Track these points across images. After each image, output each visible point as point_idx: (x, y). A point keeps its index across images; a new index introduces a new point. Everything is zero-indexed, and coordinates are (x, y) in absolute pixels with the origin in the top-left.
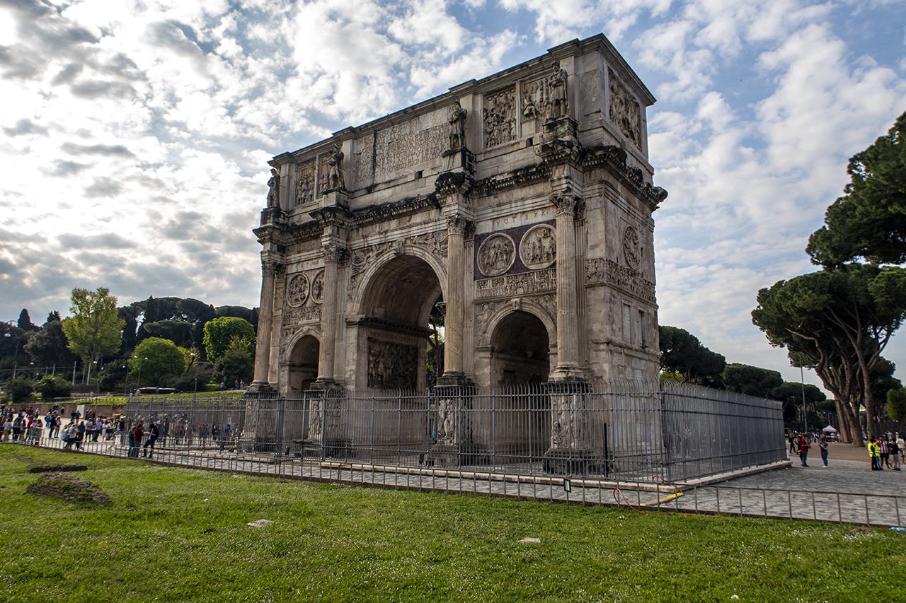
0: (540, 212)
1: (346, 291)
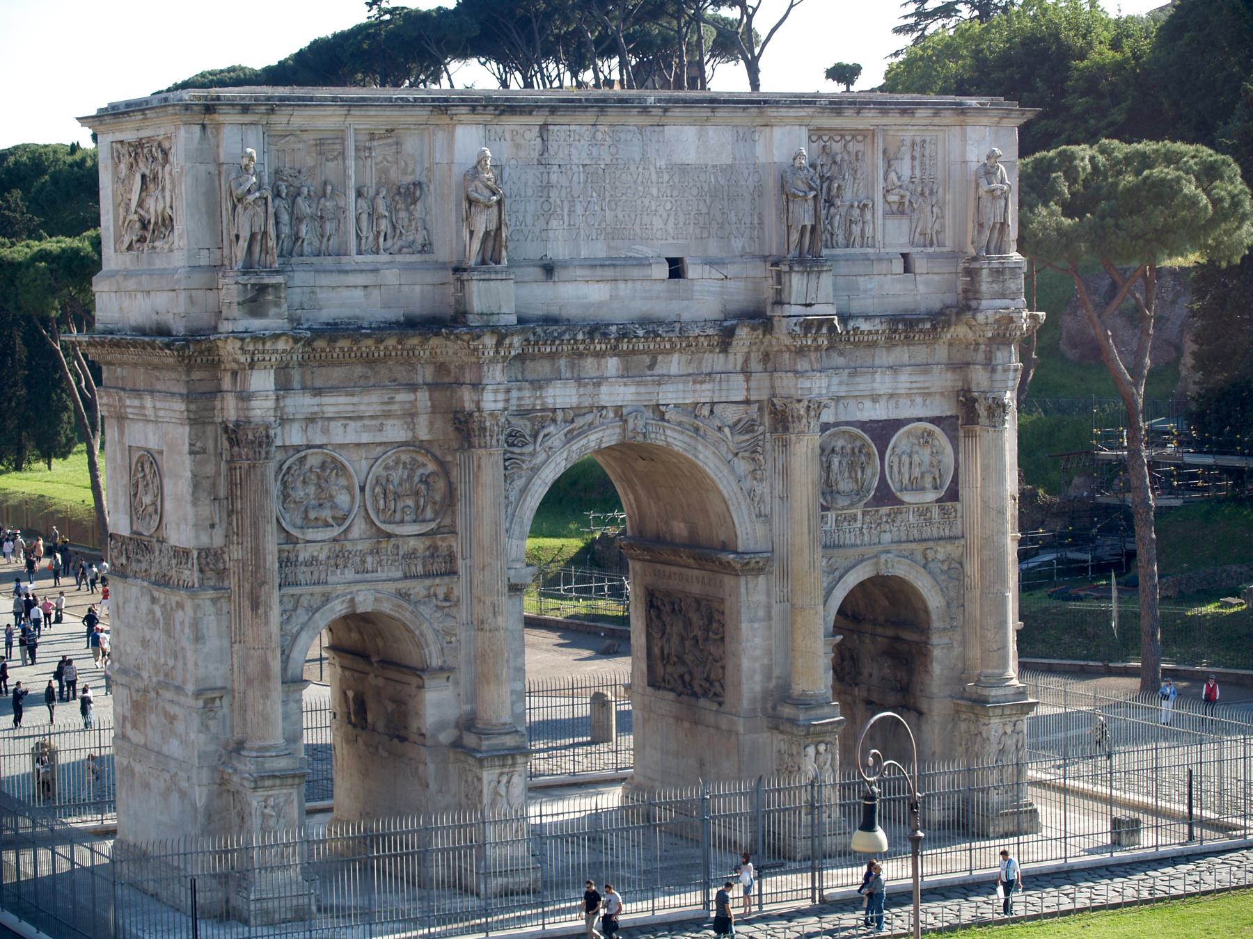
0: (919, 400)
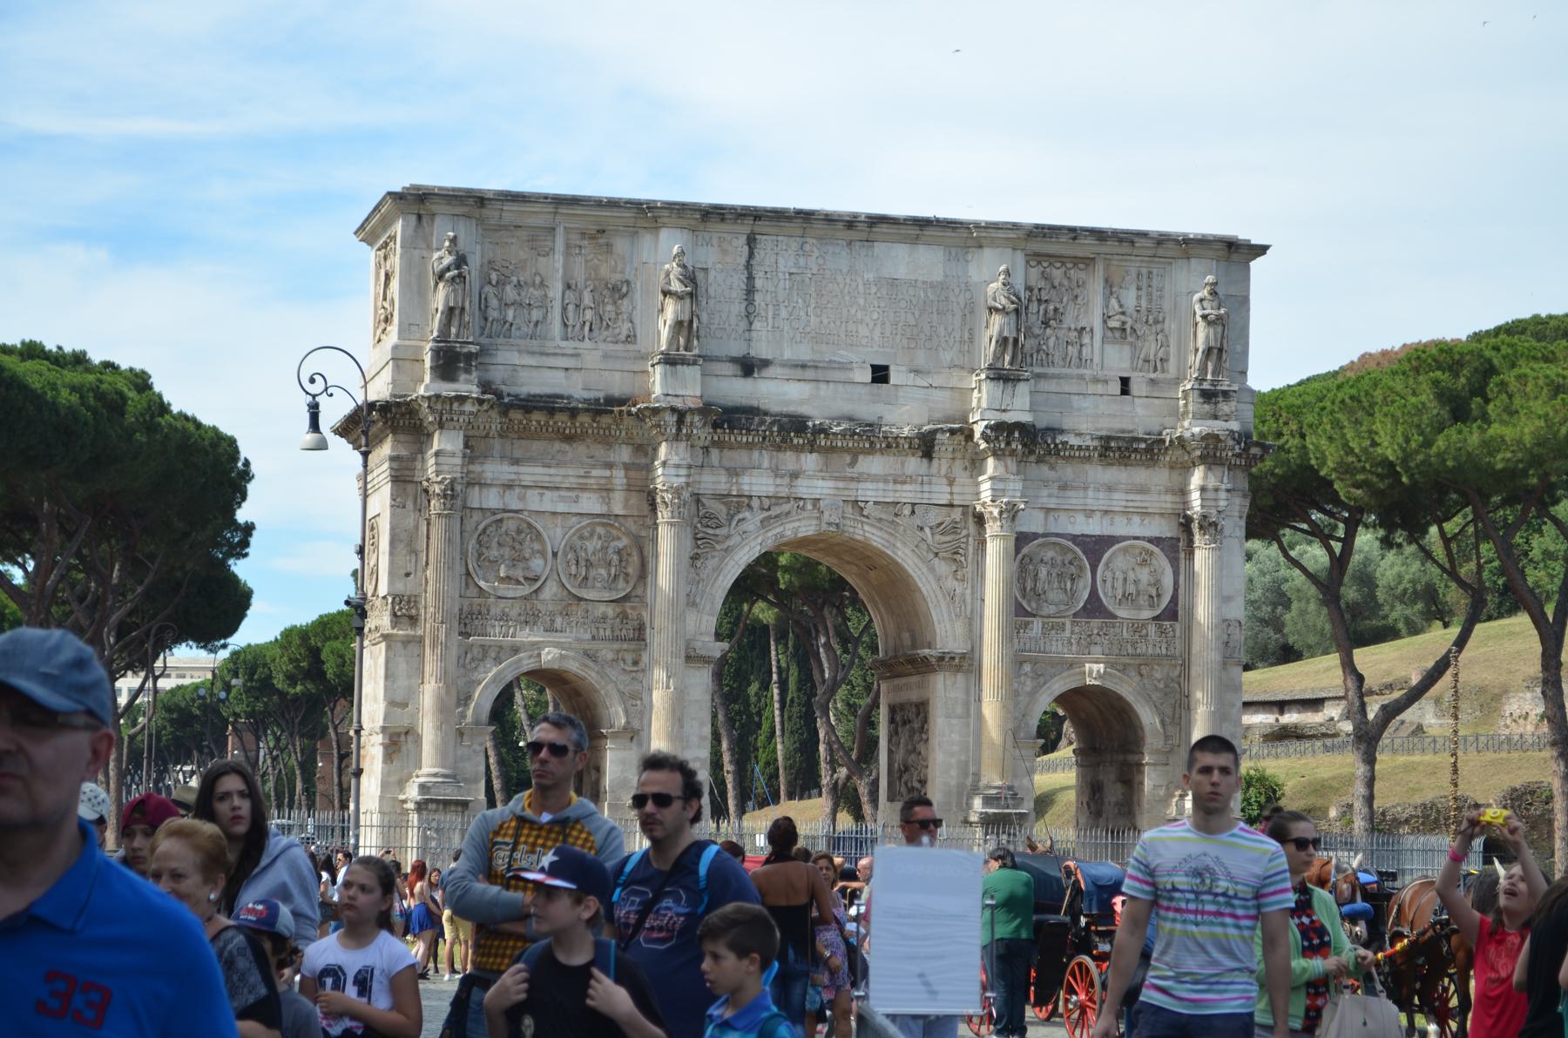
0: (1136, 519)
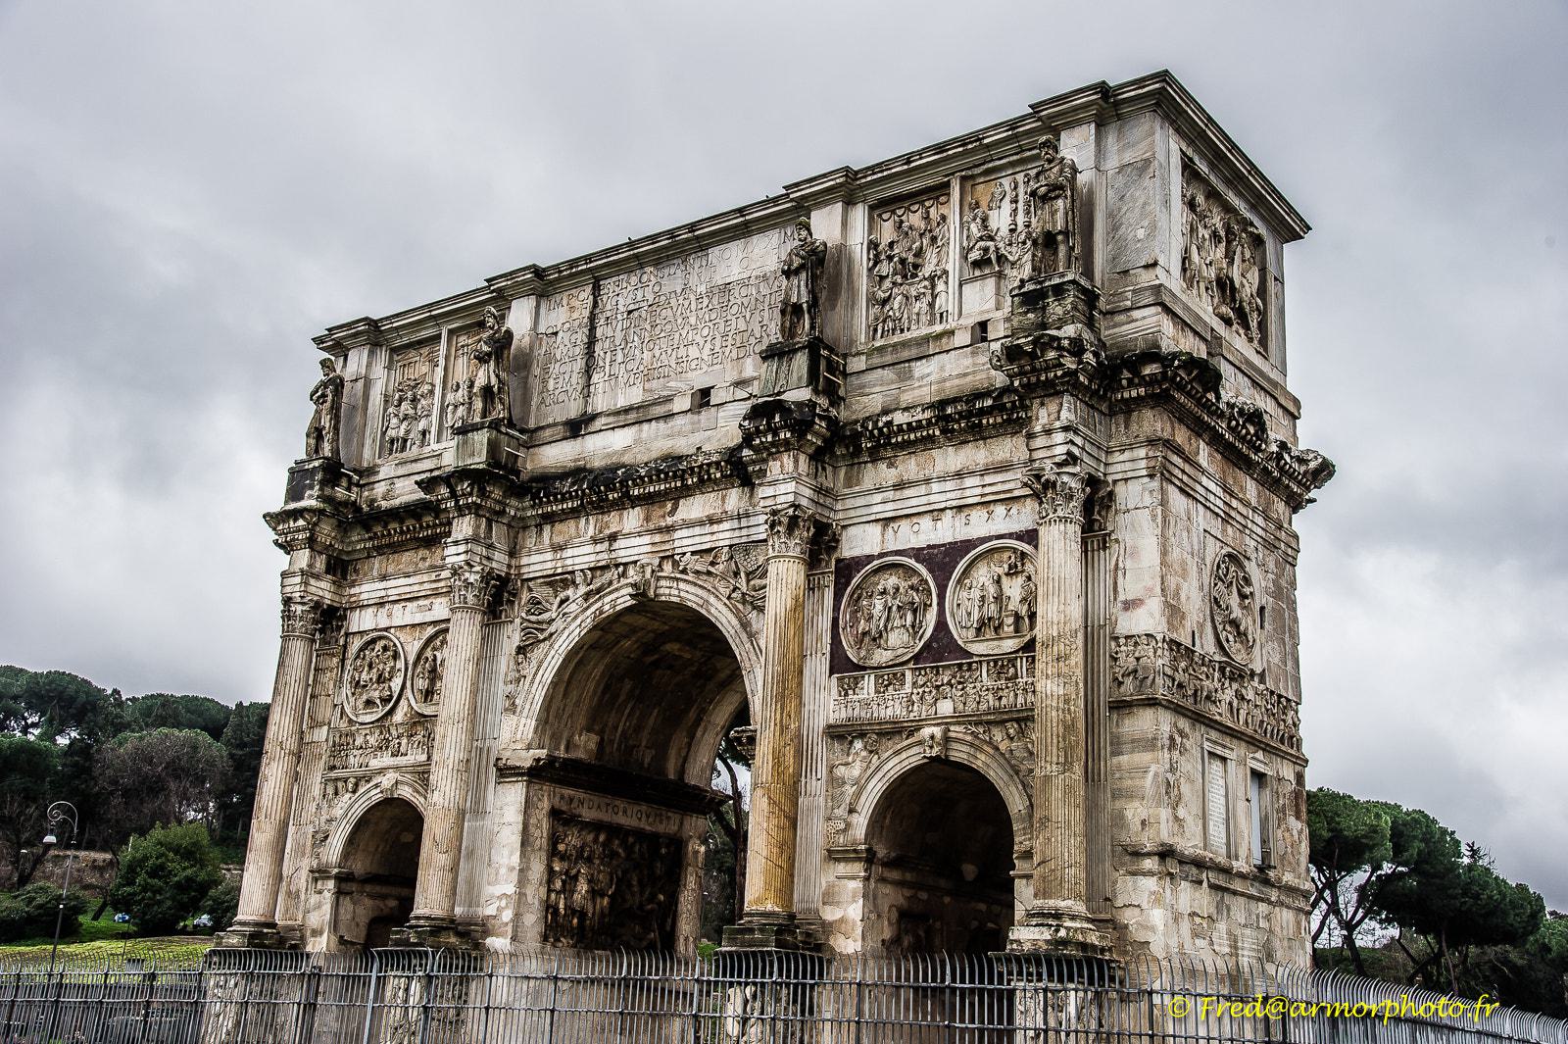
0: (1000, 510)
1: (501, 684)
